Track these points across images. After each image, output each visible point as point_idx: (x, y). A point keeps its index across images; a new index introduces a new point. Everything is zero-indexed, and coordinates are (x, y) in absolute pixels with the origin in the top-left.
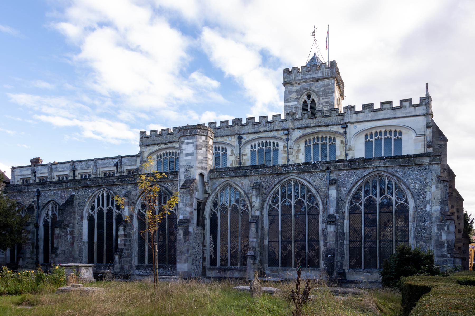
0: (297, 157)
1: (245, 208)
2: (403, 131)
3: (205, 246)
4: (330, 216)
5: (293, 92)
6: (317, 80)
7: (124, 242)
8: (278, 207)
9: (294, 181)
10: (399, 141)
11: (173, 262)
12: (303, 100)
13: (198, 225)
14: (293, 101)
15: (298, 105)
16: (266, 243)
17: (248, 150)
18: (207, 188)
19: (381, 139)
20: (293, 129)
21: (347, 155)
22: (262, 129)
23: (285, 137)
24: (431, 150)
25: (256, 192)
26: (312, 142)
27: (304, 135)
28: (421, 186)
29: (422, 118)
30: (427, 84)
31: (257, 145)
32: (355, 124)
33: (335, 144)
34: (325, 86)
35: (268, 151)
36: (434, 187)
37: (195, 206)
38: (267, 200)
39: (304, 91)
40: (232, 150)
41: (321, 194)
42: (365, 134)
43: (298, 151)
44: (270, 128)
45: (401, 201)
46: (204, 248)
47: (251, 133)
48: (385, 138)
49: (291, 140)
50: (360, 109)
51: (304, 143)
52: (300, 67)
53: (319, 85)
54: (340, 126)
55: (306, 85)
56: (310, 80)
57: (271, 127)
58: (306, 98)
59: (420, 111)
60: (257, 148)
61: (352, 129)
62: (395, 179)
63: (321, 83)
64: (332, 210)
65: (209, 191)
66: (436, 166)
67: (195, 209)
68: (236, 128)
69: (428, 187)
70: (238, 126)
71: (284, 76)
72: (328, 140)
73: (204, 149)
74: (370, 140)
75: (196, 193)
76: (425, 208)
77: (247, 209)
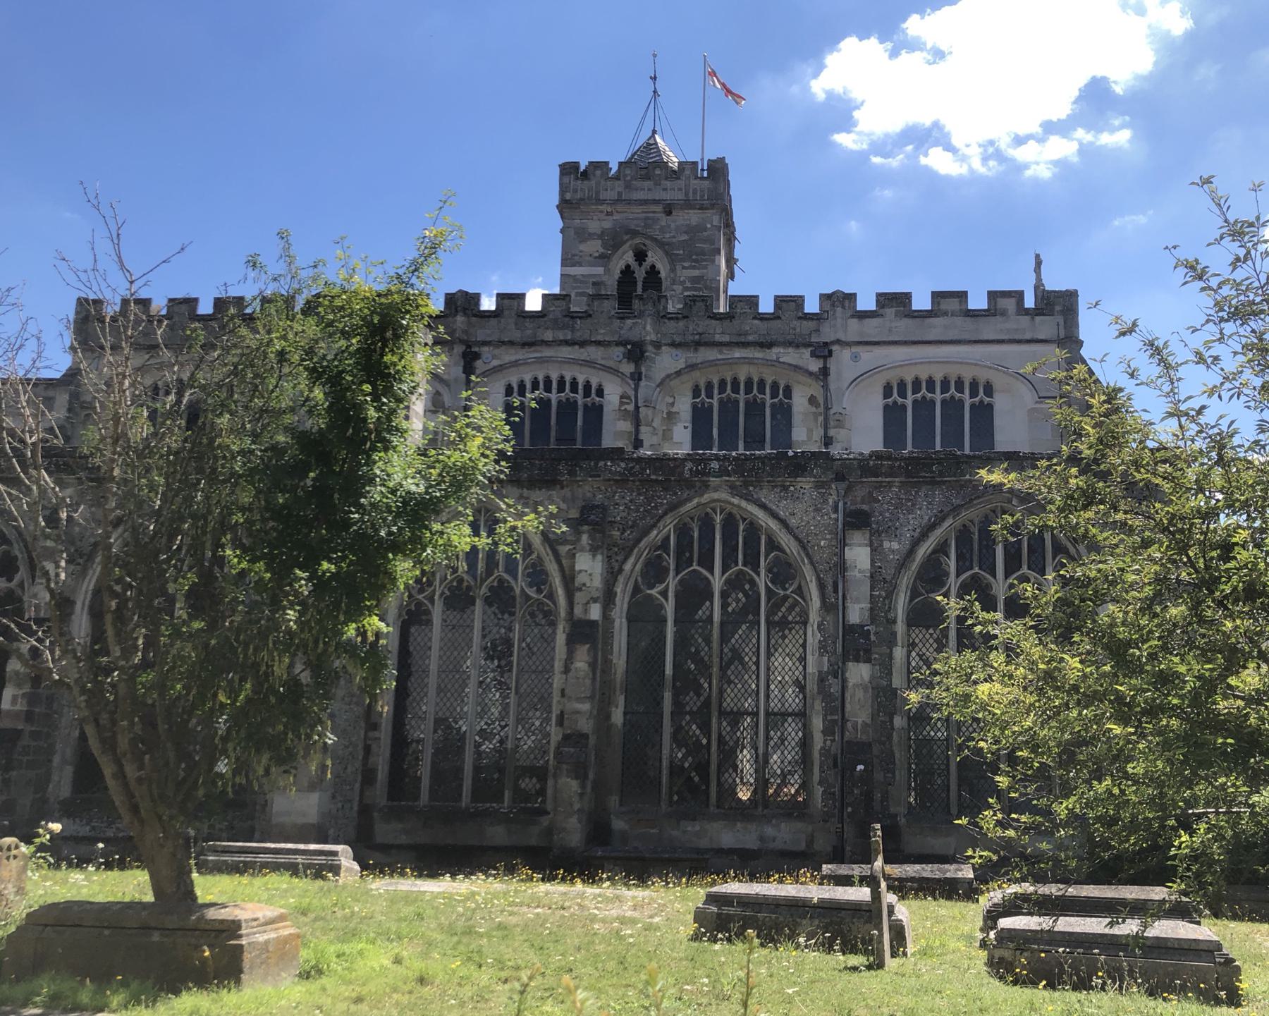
0: (667, 436)
1: (539, 591)
4: (849, 629)
5: (591, 236)
7: (30, 703)
8: (664, 593)
12: (621, 265)
15: (604, 279)
16: (618, 716)
19: (933, 402)
20: (657, 345)
21: (828, 441)
22: (549, 336)
23: (628, 368)
25: (591, 537)
26: (716, 391)
27: (691, 367)
31: (528, 386)
32: (855, 349)
33: (790, 407)
38: (628, 567)
39: (626, 237)
40: (438, 393)
41: (816, 558)
43: (671, 417)
44: (578, 334)
47: (511, 343)
48: (944, 402)
49: (649, 378)
50: (872, 306)
51: (690, 394)
53: (673, 225)
54: (807, 353)
57: (582, 330)
58: (629, 258)
59: (1047, 327)
61: (844, 364)
64: (856, 613)
70: (465, 314)
74: (900, 400)
77: (551, 596)
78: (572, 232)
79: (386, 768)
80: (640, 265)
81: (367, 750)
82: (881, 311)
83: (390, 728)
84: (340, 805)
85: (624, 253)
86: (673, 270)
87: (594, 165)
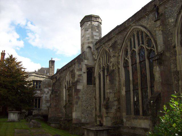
3: (96, 99)
9: (135, 30)
18: (94, 56)
46: (96, 101)
67: (84, 73)
73: (90, 30)
75: (86, 61)
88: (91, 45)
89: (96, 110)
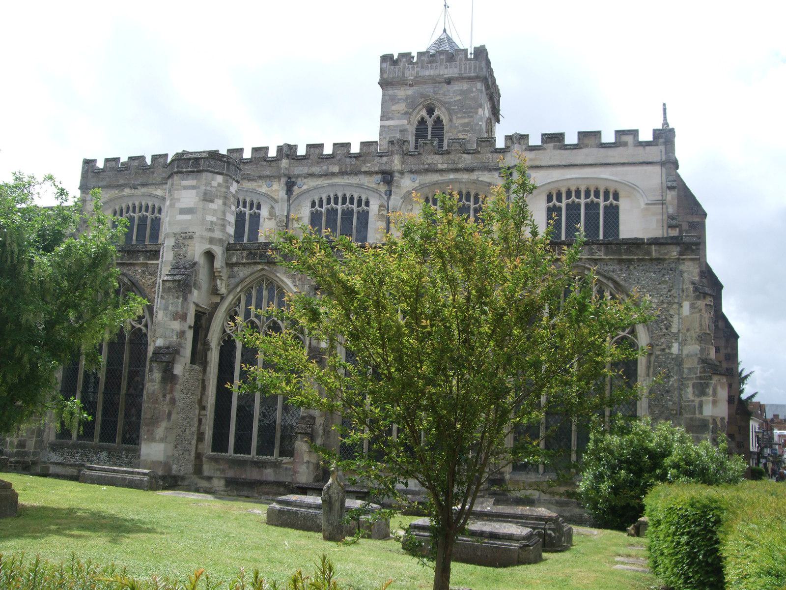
2: (621, 194)
5: (399, 101)
6: (449, 81)
10: (613, 213)
11: (132, 439)
12: (419, 118)
13: (193, 362)
14: (399, 119)
15: (408, 127)
17: (305, 212)
18: (218, 282)
19: (579, 205)
20: (402, 173)
23: (383, 188)
24: (675, 233)
28: (663, 302)
29: (657, 169)
30: (664, 105)
31: (325, 201)
34: (462, 93)
35: (347, 214)
36: (686, 305)
37: (191, 320)
40: (272, 207)
42: (547, 192)
45: (623, 331)
48: (586, 205)
52: (414, 54)
54: (496, 175)
55: (428, 89)
56: (435, 81)
58: (424, 113)
59: (655, 153)
60: (325, 206)
62: (611, 285)
63: (456, 87)
65: (223, 290)
66: (690, 263)
67: (190, 327)
68: (284, 163)
69: (675, 306)
71: (381, 69)
72: (472, 199)
74: (558, 204)
76: (670, 348)
78: (387, 98)
79: (211, 433)
80: (430, 117)
81: (200, 421)
82: (545, 145)
83: (213, 410)
84: (181, 452)
85: (420, 110)
86: (451, 120)
87: (402, 55)
88: (218, 251)
89: (200, 437)
